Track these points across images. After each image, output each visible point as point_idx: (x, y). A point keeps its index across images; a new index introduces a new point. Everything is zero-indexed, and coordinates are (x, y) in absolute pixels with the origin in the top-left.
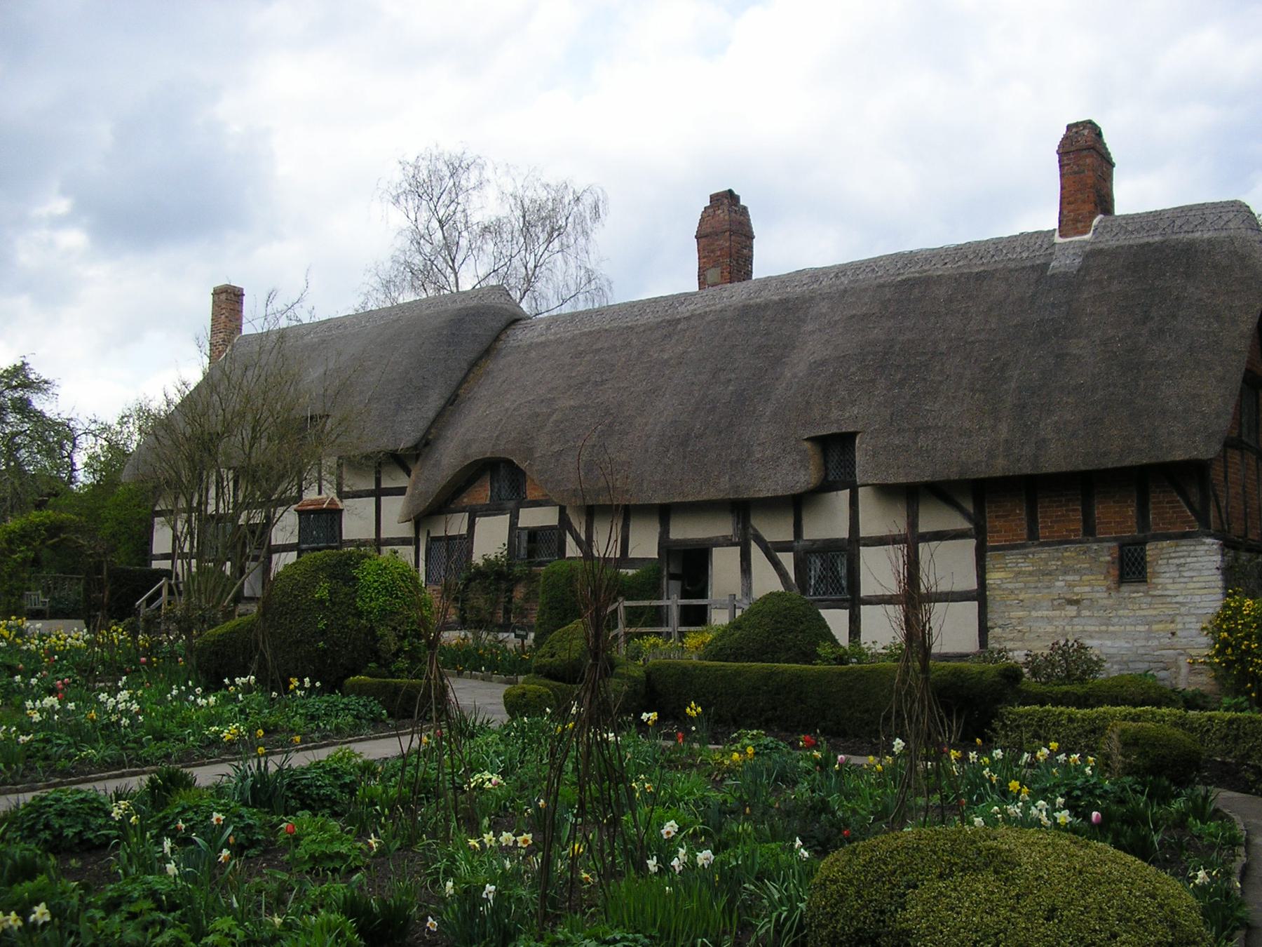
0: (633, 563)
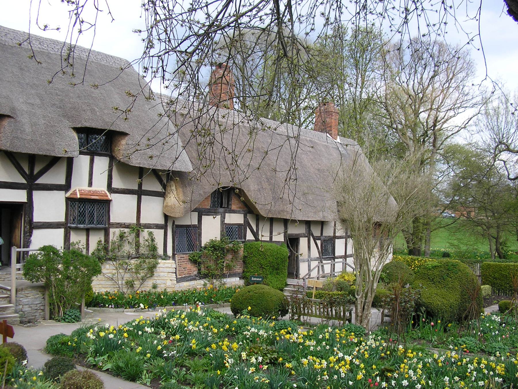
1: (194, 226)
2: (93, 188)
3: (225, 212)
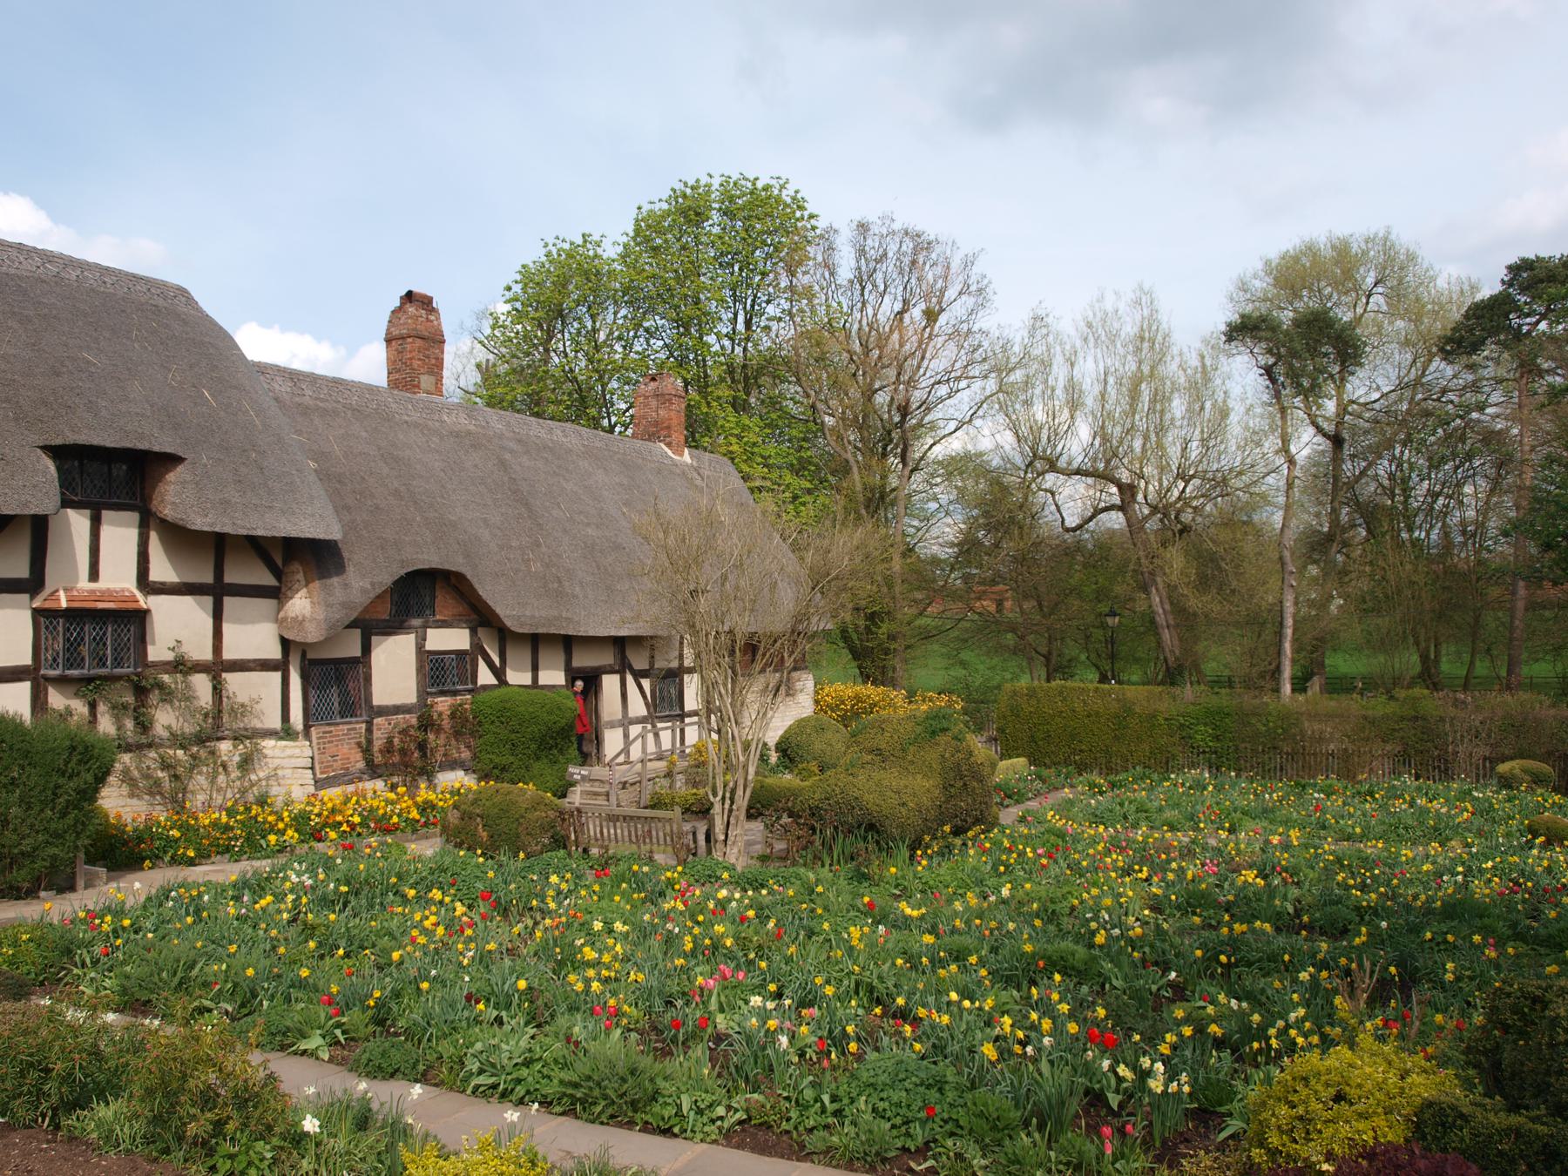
0: (544, 687)
1: (354, 661)
2: (103, 584)
3: (425, 627)
